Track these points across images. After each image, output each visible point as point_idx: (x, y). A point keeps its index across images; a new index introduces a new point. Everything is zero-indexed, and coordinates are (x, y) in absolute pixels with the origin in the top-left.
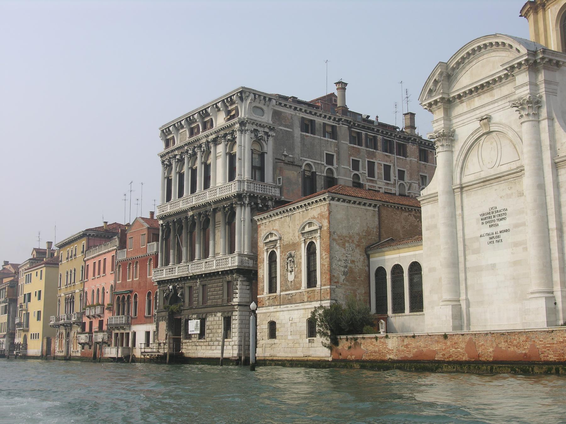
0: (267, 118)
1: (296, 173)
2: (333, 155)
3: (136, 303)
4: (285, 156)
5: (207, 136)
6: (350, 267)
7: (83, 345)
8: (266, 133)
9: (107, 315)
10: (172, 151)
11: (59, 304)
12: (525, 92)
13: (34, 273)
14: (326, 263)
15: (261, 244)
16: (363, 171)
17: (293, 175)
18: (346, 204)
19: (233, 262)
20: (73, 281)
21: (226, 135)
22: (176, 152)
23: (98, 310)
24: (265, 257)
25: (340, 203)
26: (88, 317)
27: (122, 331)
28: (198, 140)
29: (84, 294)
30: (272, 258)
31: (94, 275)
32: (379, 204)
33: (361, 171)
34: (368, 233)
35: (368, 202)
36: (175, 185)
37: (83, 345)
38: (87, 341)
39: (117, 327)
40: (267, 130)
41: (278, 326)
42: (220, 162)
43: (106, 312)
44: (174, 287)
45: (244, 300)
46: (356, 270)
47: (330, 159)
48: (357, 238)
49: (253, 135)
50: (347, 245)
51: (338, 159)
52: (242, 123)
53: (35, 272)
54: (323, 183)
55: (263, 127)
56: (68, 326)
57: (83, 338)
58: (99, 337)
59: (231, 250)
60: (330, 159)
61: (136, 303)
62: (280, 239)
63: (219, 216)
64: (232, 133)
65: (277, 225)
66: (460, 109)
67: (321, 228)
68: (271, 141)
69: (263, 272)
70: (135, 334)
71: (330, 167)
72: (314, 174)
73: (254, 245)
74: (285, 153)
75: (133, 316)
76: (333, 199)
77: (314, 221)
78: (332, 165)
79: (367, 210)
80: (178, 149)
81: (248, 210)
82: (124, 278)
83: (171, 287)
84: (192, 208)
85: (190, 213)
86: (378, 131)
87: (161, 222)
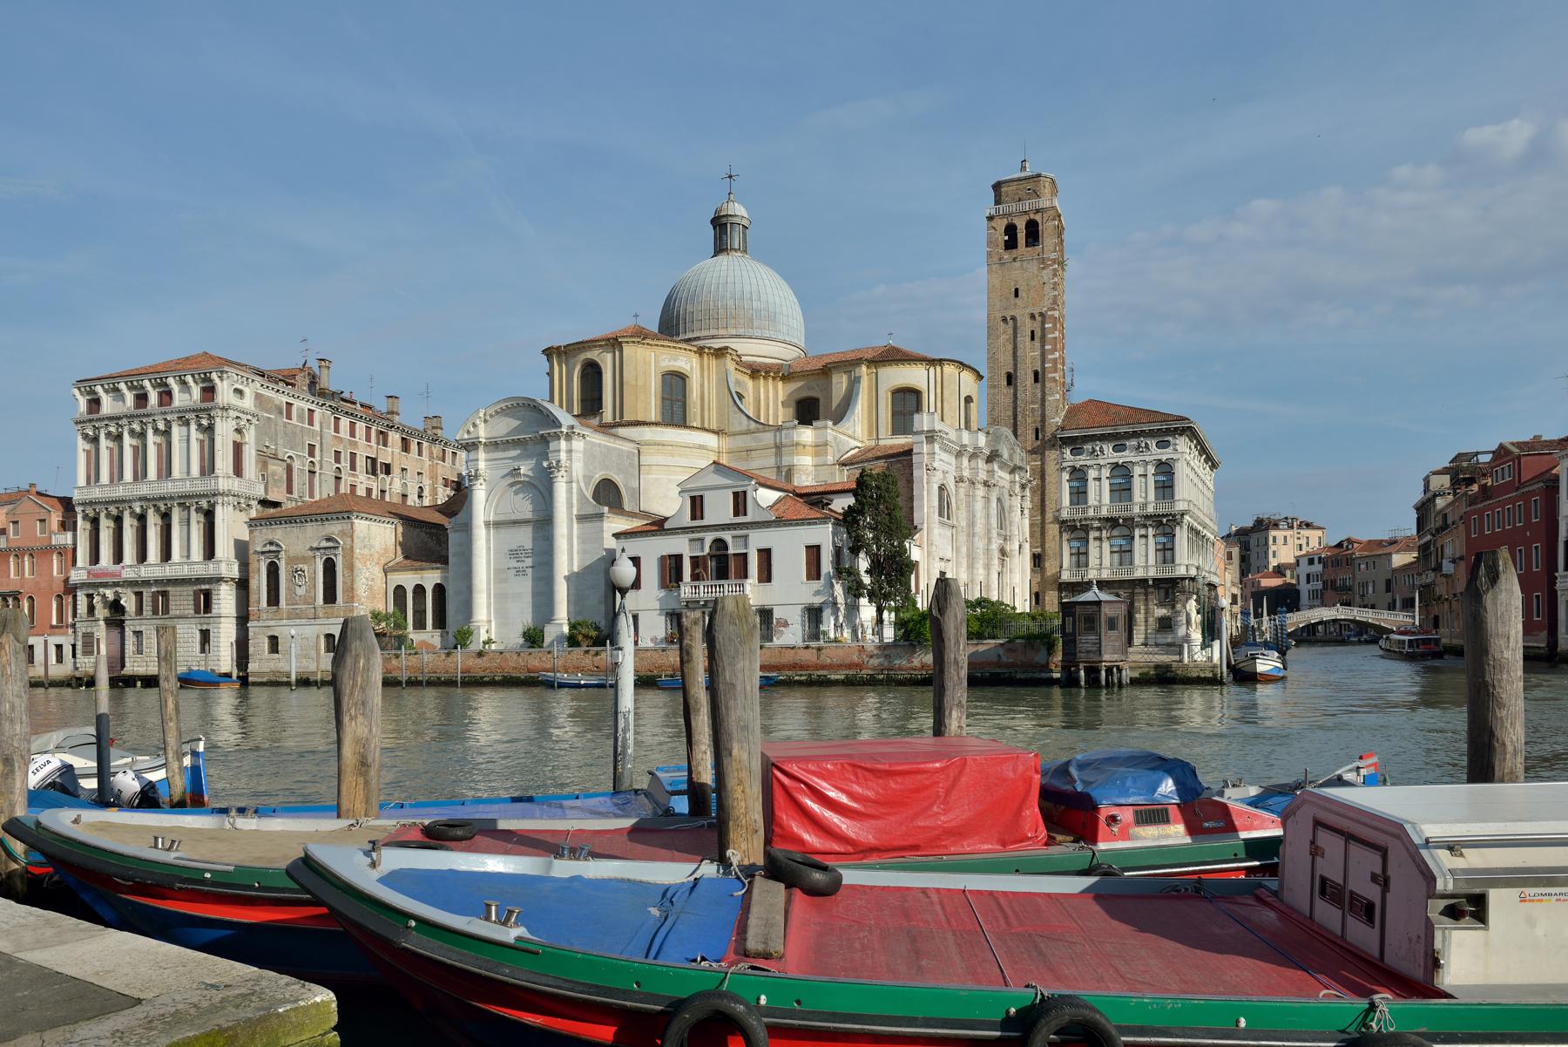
16: (345, 464)
18: (368, 522)
25: (363, 522)
33: (343, 464)
34: (386, 550)
40: (249, 417)
48: (377, 556)
49: (234, 422)
50: (368, 563)
71: (312, 459)
78: (314, 457)
79: (385, 528)
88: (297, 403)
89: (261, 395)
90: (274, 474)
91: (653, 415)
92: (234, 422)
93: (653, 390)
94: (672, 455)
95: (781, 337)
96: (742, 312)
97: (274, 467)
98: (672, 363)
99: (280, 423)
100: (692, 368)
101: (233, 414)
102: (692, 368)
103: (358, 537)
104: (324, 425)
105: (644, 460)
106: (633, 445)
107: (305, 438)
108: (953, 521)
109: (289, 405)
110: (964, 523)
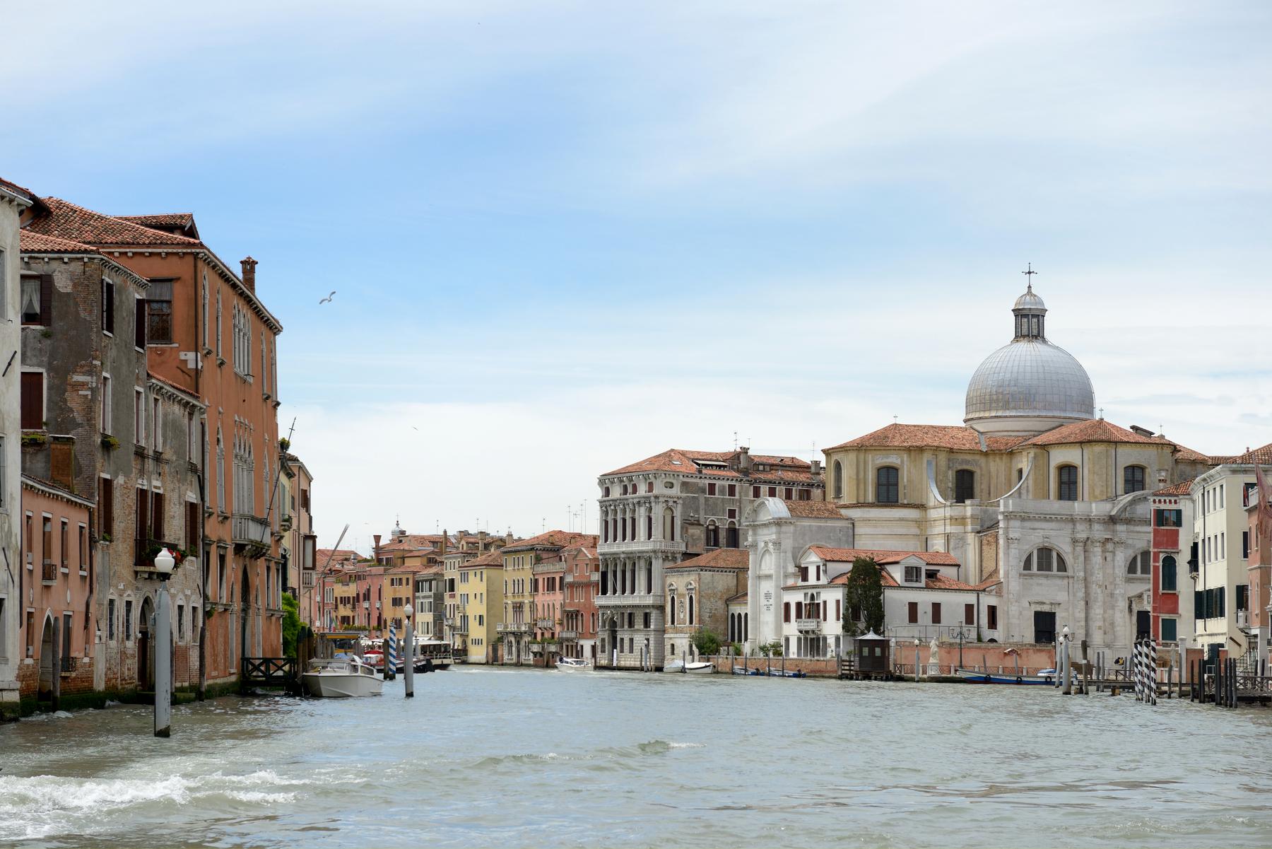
0: (676, 491)
1: (699, 531)
2: (735, 510)
3: (582, 620)
4: (692, 517)
5: (633, 498)
6: (714, 613)
7: (535, 654)
8: (675, 502)
9: (558, 629)
10: (608, 501)
11: (506, 612)
12: (774, 537)
13: (471, 576)
14: (697, 613)
15: (667, 590)
17: (697, 532)
18: (711, 573)
19: (649, 601)
20: (521, 591)
21: (645, 503)
22: (611, 503)
23: (550, 624)
24: (669, 599)
26: (540, 628)
27: (571, 643)
28: (627, 499)
29: (533, 606)
30: (673, 599)
31: (544, 591)
32: (736, 570)
34: (728, 590)
35: (728, 570)
36: (611, 525)
37: (535, 654)
38: (540, 650)
39: (568, 640)
41: (675, 647)
42: (642, 519)
43: (557, 626)
44: (612, 612)
45: (658, 627)
46: (718, 615)
47: (732, 514)
48: (720, 594)
49: (664, 505)
50: (712, 599)
51: (740, 513)
52: (656, 497)
53: (474, 571)
54: (725, 534)
55: (673, 497)
56: (518, 636)
57: (536, 648)
58: (553, 648)
59: (649, 591)
60: (732, 514)
61: (582, 620)
62: (677, 589)
63: (642, 563)
64: (650, 503)
65: (675, 579)
66: (760, 531)
67: (695, 587)
68: (679, 506)
69: (668, 609)
70: (582, 646)
72: (717, 528)
73: (663, 590)
74: (692, 515)
75: (580, 632)
76: (702, 570)
77: (692, 582)
79: (727, 575)
80: (612, 500)
81: (661, 561)
82: (572, 598)
83: (609, 612)
84: (623, 553)
85: (622, 556)
86: (780, 483)
87: (600, 557)
88: (718, 483)
89: (688, 483)
90: (692, 536)
91: (871, 498)
92: (664, 505)
93: (870, 480)
94: (876, 527)
95: (1036, 414)
96: (1001, 397)
97: (693, 531)
98: (883, 461)
99: (702, 501)
100: (902, 462)
101: (661, 499)
102: (902, 462)
103: (703, 583)
104: (742, 494)
105: (858, 530)
106: (847, 522)
107: (726, 505)
108: (1070, 573)
109: (712, 487)
110: (1082, 574)
